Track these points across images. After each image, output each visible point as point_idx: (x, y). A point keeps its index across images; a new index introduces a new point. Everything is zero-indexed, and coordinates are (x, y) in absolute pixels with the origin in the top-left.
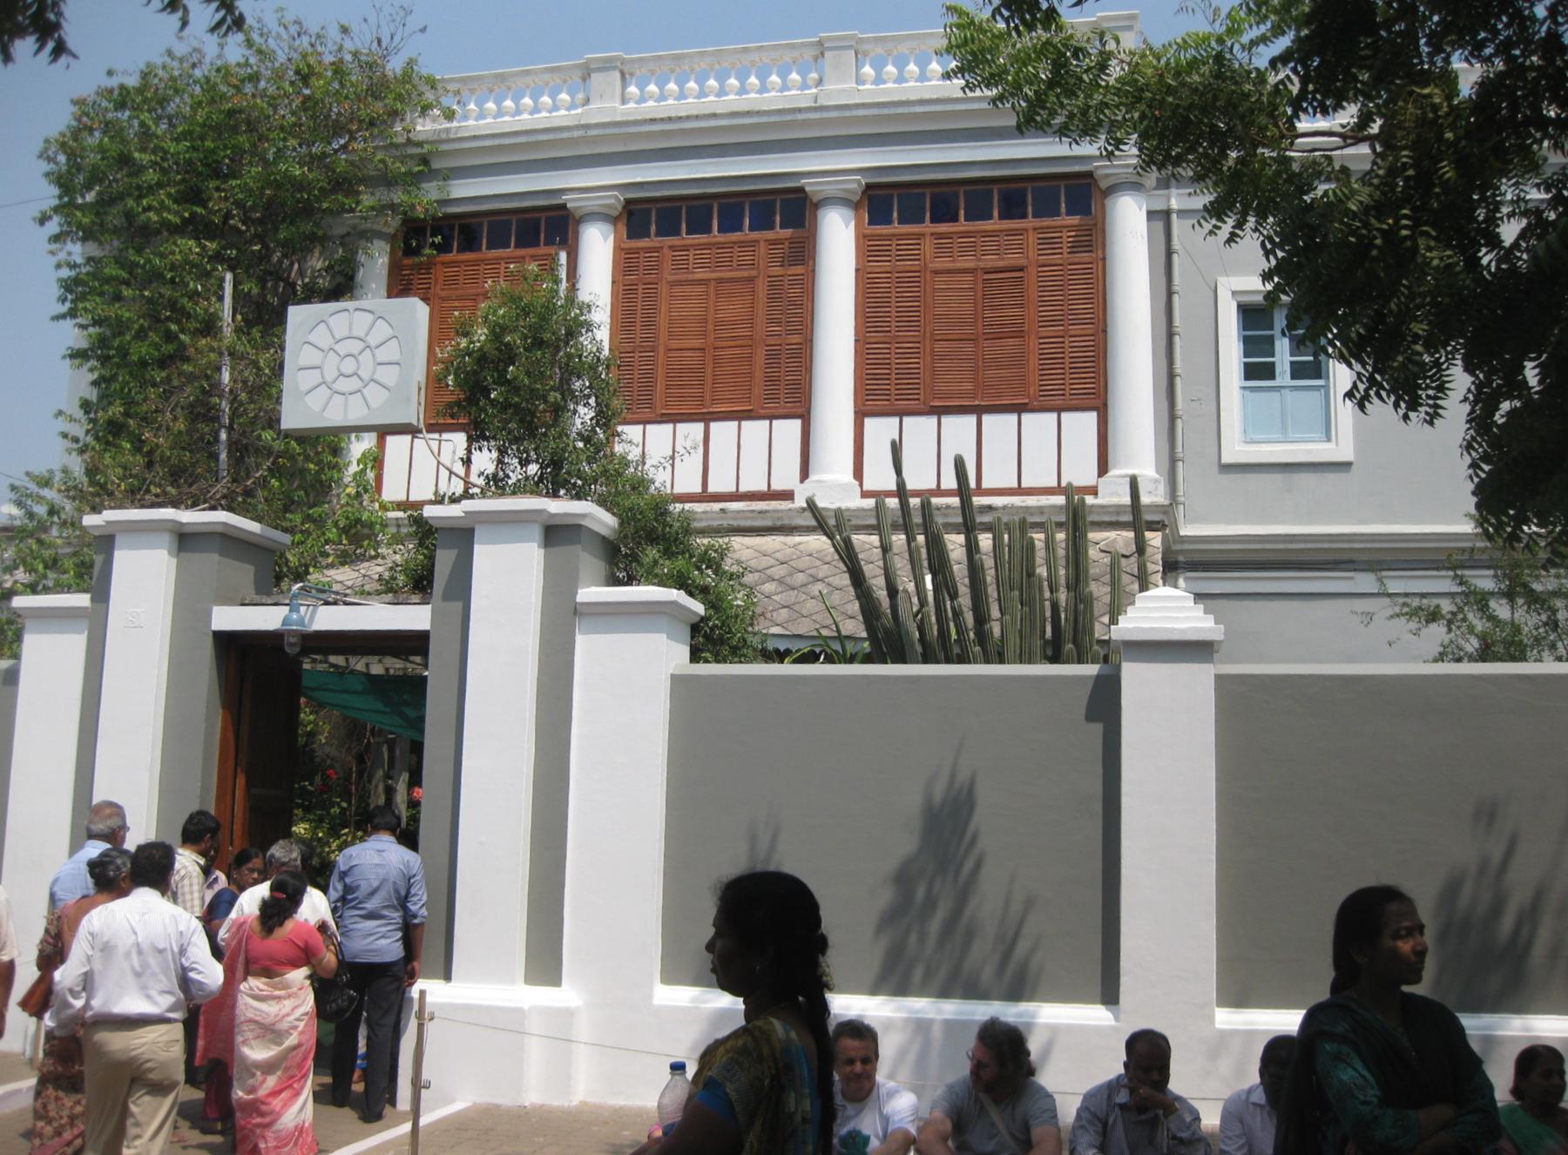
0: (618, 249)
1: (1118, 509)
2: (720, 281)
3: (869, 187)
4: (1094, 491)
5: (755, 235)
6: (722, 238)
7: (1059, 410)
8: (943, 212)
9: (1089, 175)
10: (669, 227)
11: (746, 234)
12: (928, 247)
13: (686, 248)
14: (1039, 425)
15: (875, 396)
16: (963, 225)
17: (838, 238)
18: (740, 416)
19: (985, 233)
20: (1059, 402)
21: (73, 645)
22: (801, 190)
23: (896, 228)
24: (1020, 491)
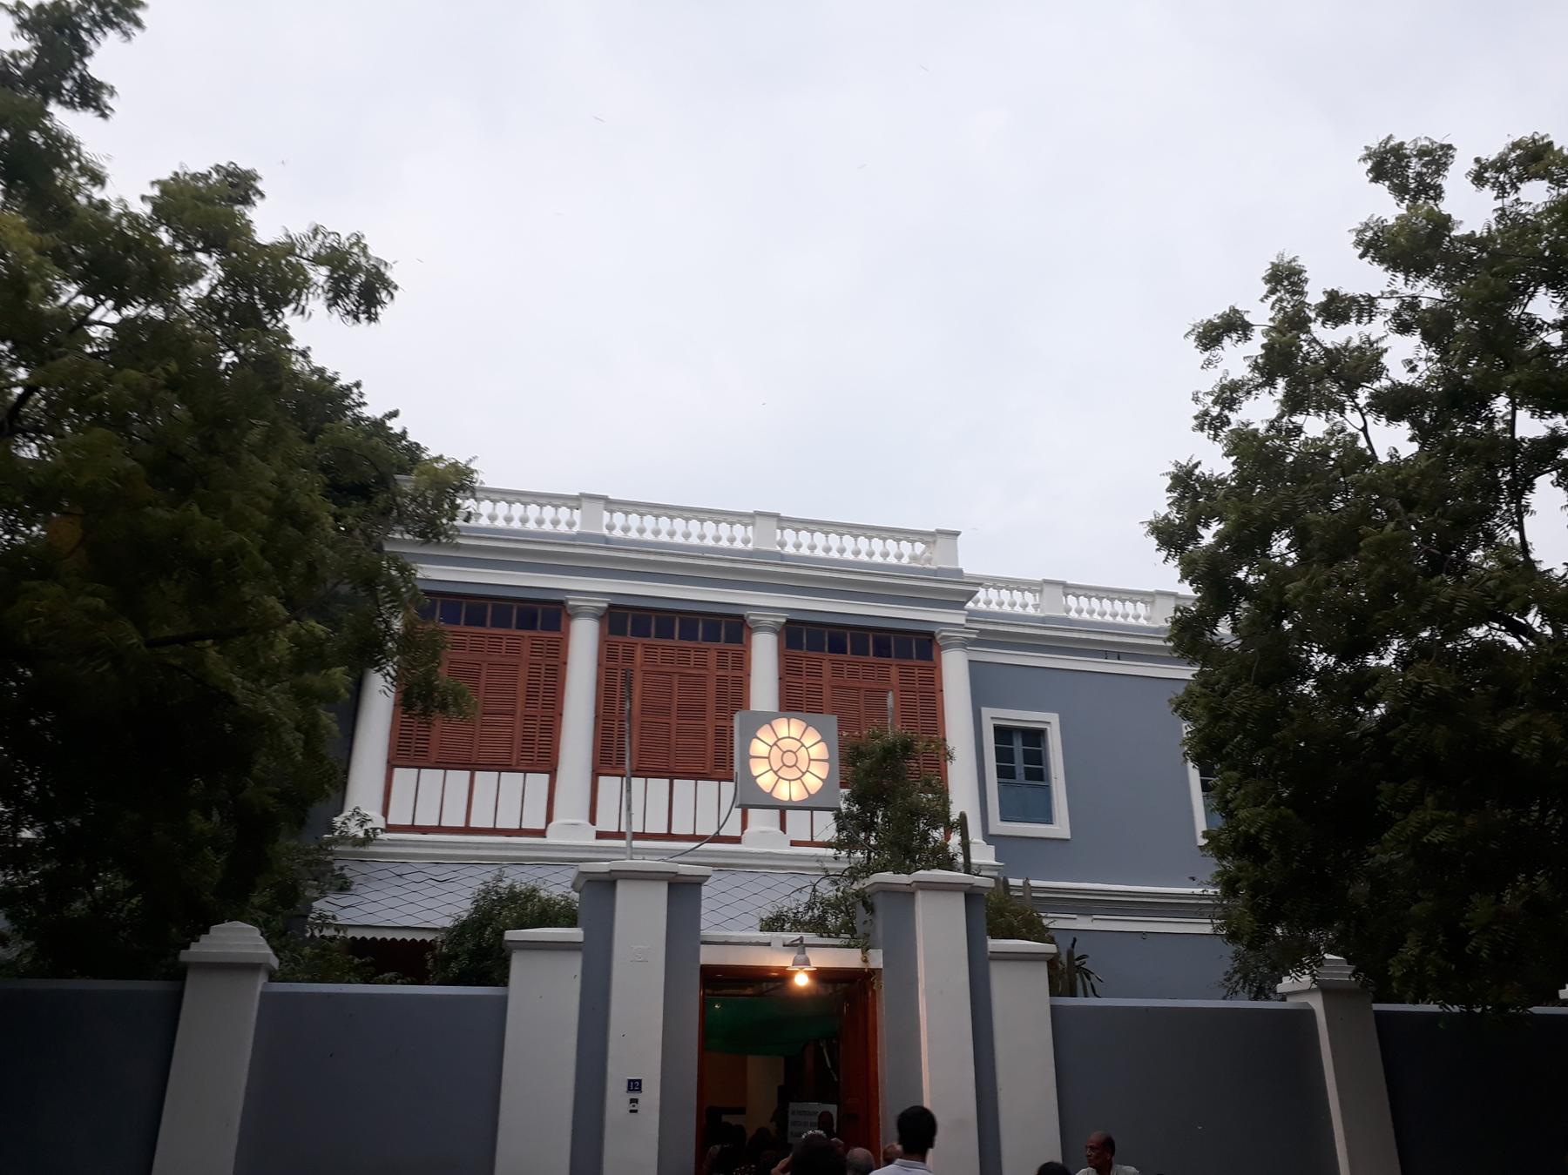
2: (682, 674)
3: (789, 621)
5: (708, 644)
8: (837, 646)
9: (932, 634)
10: (641, 630)
12: (827, 667)
13: (655, 647)
15: (606, 760)
16: (848, 656)
17: (764, 653)
18: (697, 776)
19: (865, 664)
21: (568, 974)
22: (741, 617)
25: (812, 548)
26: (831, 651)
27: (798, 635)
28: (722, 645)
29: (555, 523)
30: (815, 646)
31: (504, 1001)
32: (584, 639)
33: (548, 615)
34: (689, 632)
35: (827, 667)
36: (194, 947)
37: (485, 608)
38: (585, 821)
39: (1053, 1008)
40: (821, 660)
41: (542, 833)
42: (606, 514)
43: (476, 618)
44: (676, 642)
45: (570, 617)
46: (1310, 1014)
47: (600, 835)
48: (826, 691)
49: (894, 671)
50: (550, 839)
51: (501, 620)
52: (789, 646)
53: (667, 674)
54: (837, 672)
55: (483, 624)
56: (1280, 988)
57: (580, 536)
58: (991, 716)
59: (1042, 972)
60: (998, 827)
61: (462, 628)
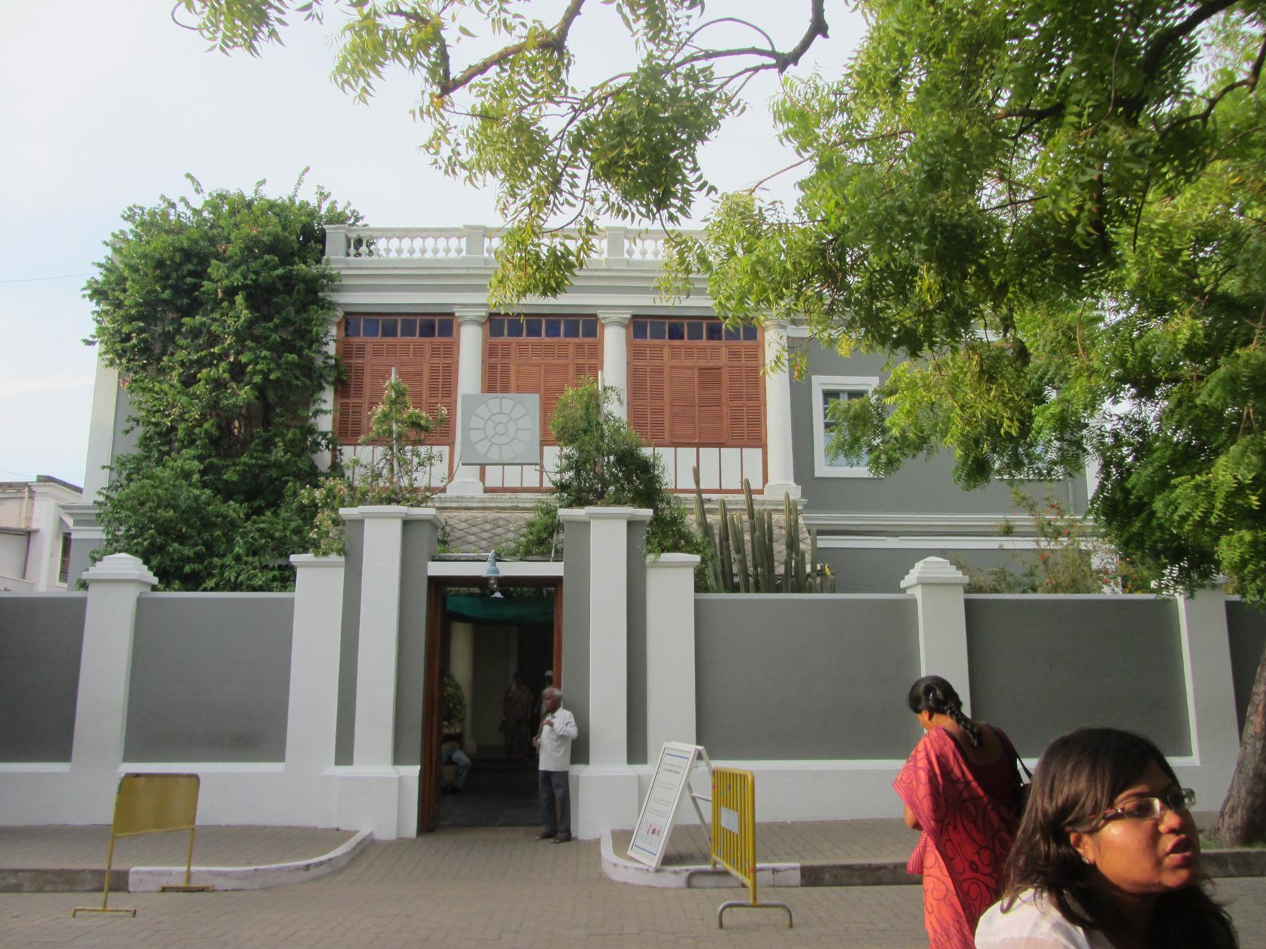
0: (485, 342)
1: (779, 503)
2: (547, 365)
3: (634, 317)
4: (761, 492)
5: (568, 340)
6: (548, 340)
7: (742, 447)
8: (676, 333)
10: (515, 330)
11: (562, 339)
12: (666, 352)
14: (731, 454)
16: (686, 341)
20: (741, 442)
22: (595, 315)
23: (649, 341)
24: (720, 491)
25: (644, 253)
26: (670, 338)
27: (641, 326)
28: (580, 340)
29: (447, 251)
30: (657, 335)
31: (292, 600)
32: (470, 342)
33: (438, 325)
34: (553, 331)
35: (666, 352)
36: (92, 570)
37: (396, 322)
38: (476, 480)
39: (697, 602)
40: (662, 347)
41: (443, 490)
42: (487, 240)
43: (389, 331)
44: (544, 339)
45: (460, 325)
46: (914, 602)
47: (486, 490)
48: (666, 370)
49: (724, 352)
50: (449, 493)
51: (408, 331)
52: (636, 336)
53: (539, 365)
54: (675, 355)
55: (394, 334)
56: (903, 584)
57: (464, 259)
58: (820, 383)
59: (689, 578)
60: (822, 469)
61: (379, 338)
